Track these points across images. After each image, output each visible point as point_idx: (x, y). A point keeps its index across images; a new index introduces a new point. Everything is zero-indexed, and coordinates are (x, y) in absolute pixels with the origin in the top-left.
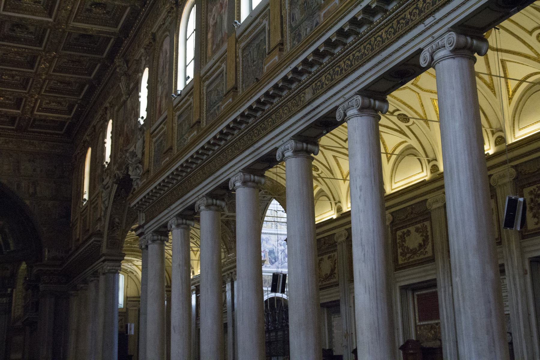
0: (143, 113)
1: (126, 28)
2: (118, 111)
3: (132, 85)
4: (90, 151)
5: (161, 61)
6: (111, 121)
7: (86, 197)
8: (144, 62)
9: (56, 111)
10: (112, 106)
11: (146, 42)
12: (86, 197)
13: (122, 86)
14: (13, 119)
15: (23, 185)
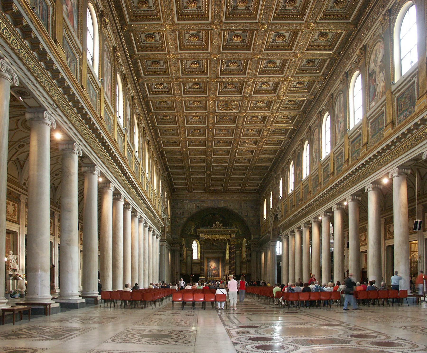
0: (281, 195)
1: (274, 163)
2: (274, 189)
3: (278, 182)
4: (266, 200)
5: (285, 177)
6: (272, 192)
7: (265, 217)
8: (281, 176)
9: (253, 186)
10: (272, 187)
11: (281, 169)
12: (265, 217)
13: (274, 181)
14: (238, 190)
15: (243, 212)
